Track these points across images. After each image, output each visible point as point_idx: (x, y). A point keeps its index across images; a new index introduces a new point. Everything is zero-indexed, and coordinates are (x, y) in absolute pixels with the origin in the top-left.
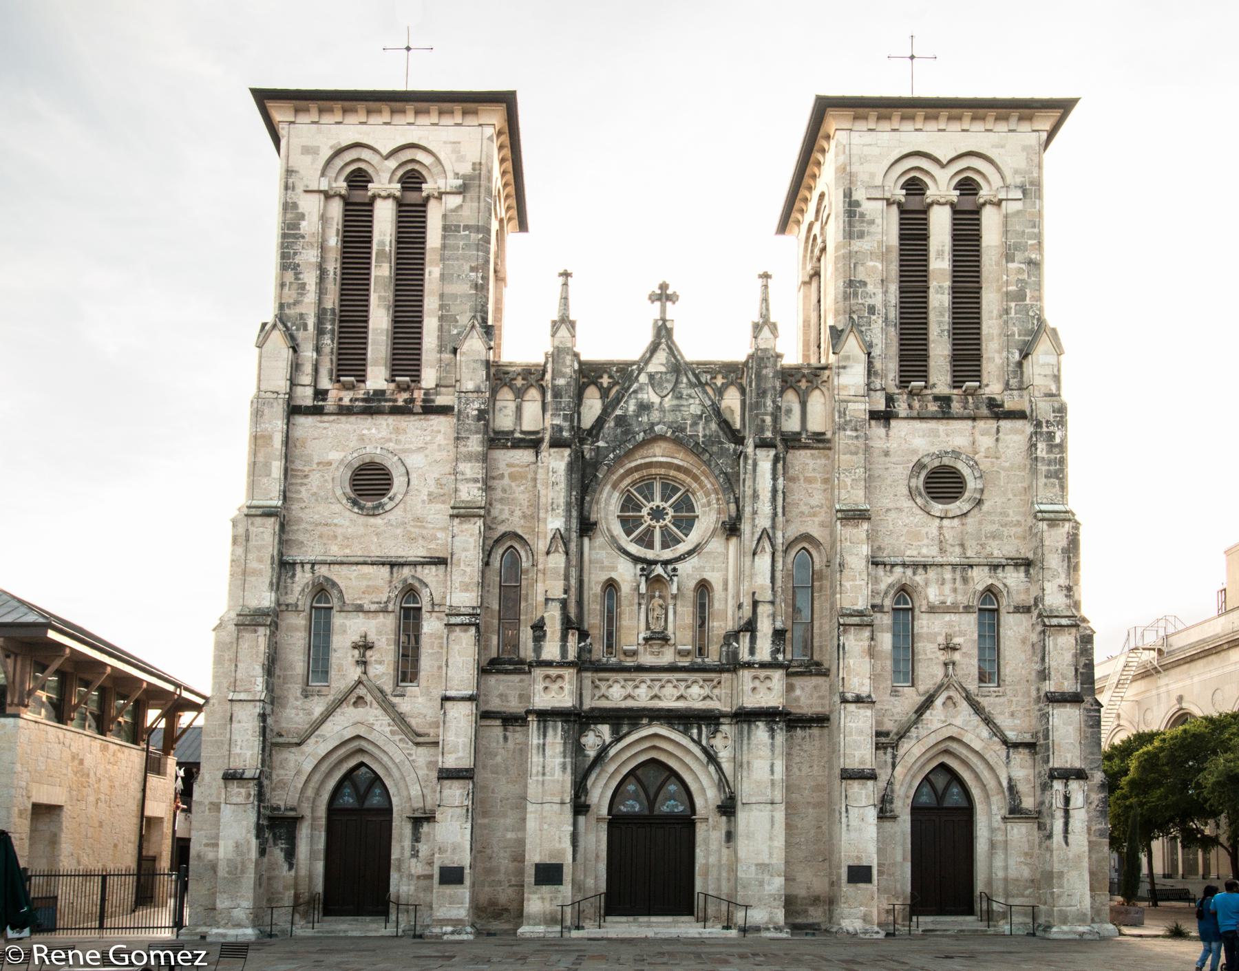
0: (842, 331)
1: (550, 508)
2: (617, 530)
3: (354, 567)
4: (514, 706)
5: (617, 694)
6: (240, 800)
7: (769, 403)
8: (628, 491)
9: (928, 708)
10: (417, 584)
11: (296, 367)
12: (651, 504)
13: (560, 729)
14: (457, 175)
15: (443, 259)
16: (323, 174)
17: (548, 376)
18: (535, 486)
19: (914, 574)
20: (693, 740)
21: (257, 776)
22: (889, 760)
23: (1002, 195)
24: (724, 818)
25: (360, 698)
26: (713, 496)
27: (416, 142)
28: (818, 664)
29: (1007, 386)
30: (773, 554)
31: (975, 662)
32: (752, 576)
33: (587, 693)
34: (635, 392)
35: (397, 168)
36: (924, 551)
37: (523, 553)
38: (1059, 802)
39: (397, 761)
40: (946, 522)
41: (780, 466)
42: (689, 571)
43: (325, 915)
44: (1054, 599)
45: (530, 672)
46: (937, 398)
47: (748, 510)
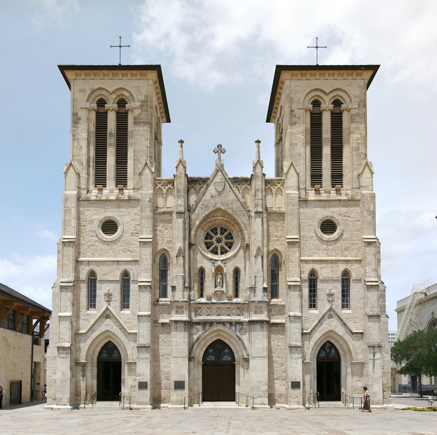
1: (177, 238)
2: (204, 246)
8: (208, 230)
16: (87, 101)
21: (69, 346)
23: (350, 107)
24: (245, 363)
27: (122, 87)
33: (193, 314)
35: (116, 98)
39: (122, 340)
43: (97, 401)
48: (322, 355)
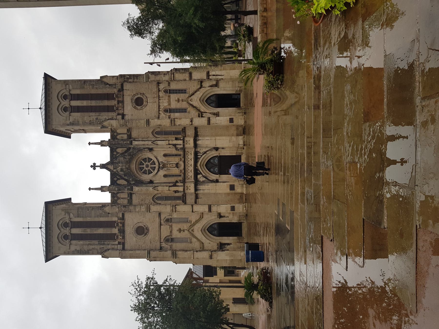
3: (161, 233)
4: (193, 197)
5: (191, 174)
6: (216, 255)
7: (121, 142)
9: (193, 105)
10: (165, 219)
11: (113, 249)
12: (145, 167)
14: (65, 215)
15: (86, 217)
17: (115, 192)
18: (141, 194)
19: (161, 108)
20: (201, 157)
22: (205, 113)
24: (219, 150)
25: (192, 230)
26: (143, 154)
28: (183, 129)
29: (115, 88)
30: (157, 140)
31: (182, 94)
32: (163, 145)
33: (190, 180)
36: (155, 106)
37: (157, 196)
38: (214, 77)
40: (148, 102)
42: (162, 159)
44: (167, 78)
45: (186, 193)
46: (118, 103)
47: (147, 146)
48: (213, 105)
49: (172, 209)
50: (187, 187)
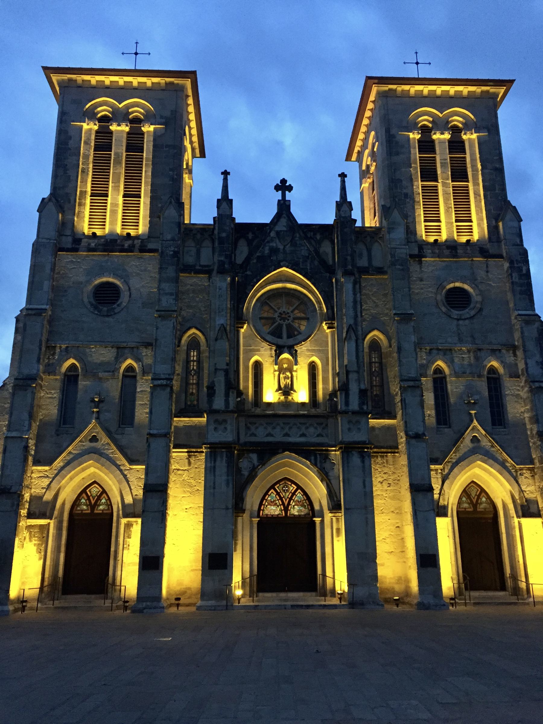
0: (390, 207)
1: (217, 311)
13: (225, 456)
17: (216, 232)
34: (268, 242)
36: (449, 340)
40: (461, 322)
41: (358, 286)
48: (466, 505)
49: (163, 376)
50: (225, 421)
